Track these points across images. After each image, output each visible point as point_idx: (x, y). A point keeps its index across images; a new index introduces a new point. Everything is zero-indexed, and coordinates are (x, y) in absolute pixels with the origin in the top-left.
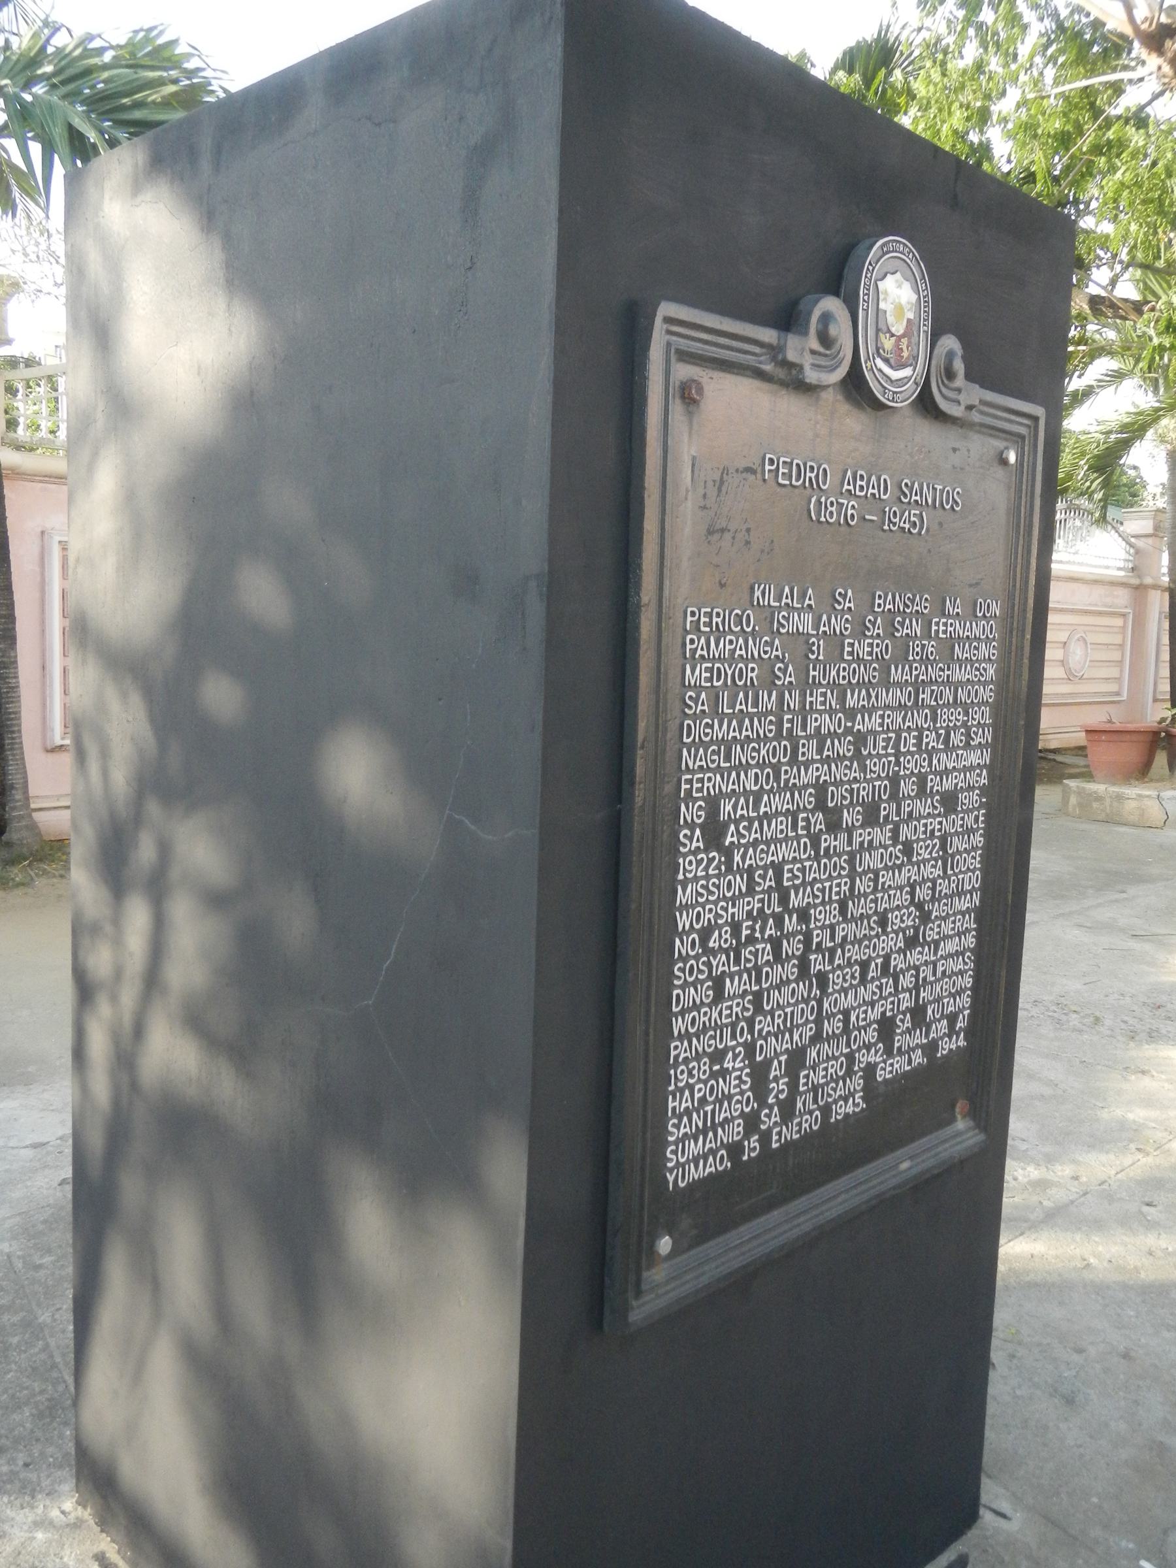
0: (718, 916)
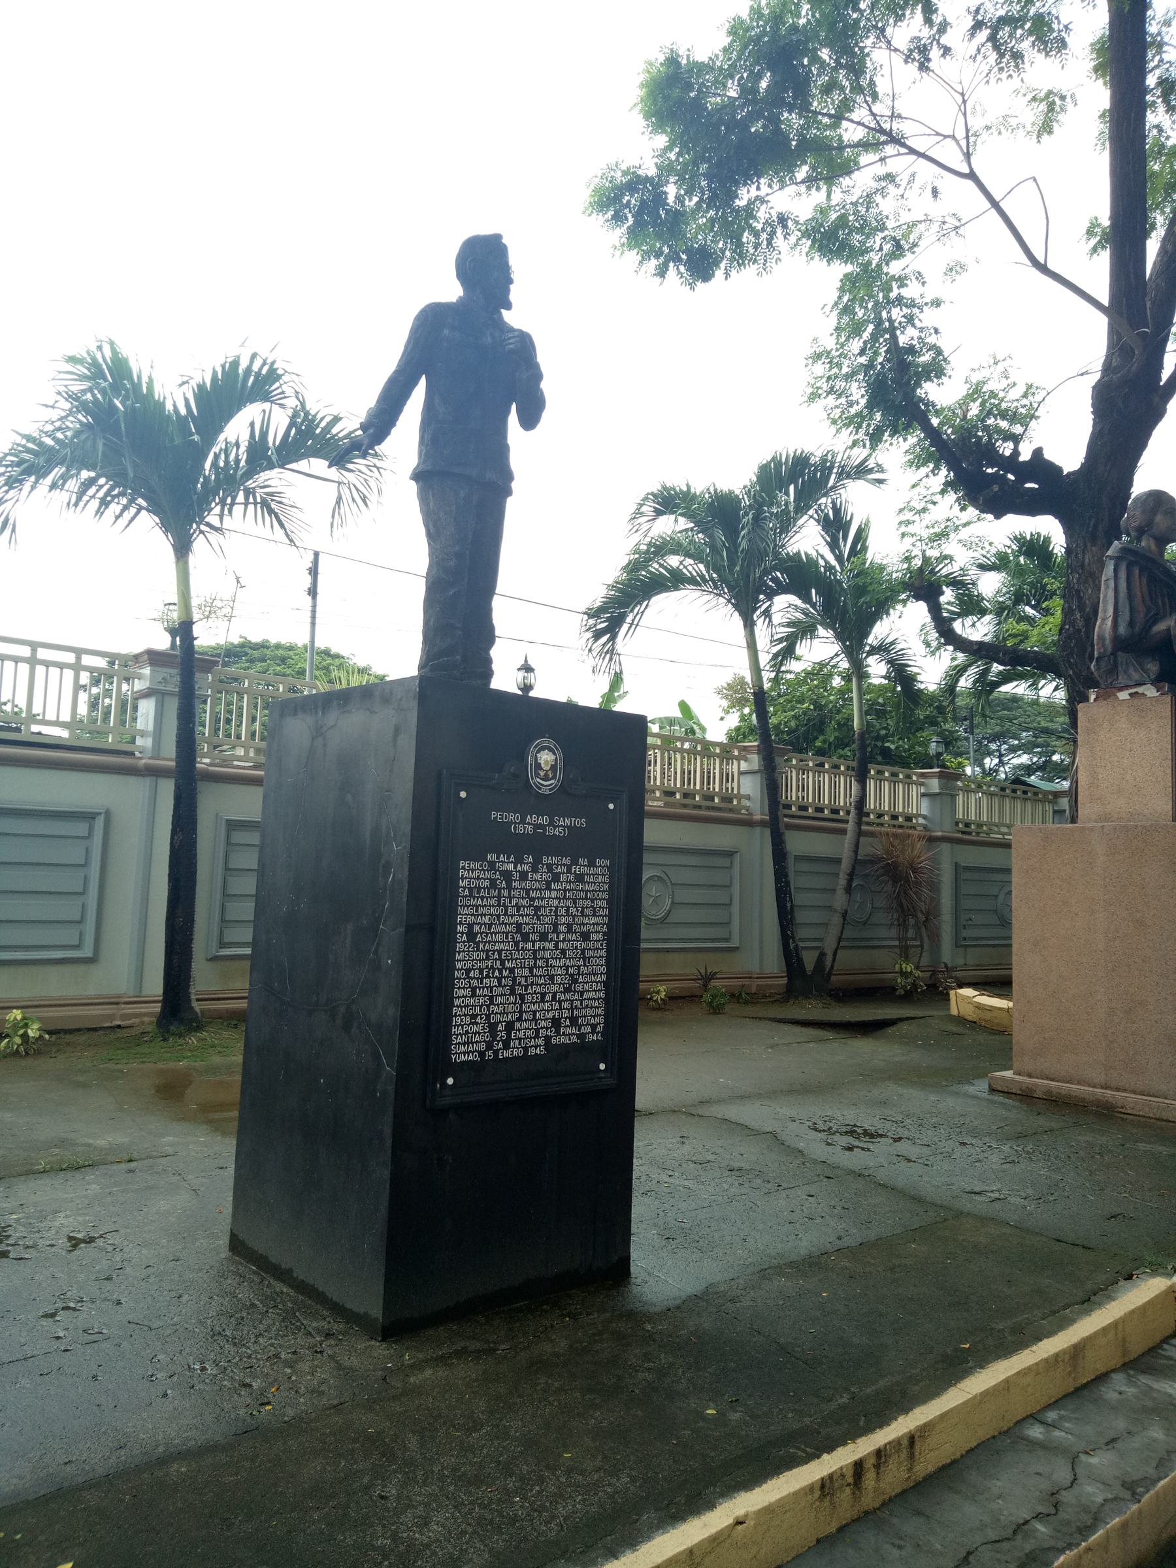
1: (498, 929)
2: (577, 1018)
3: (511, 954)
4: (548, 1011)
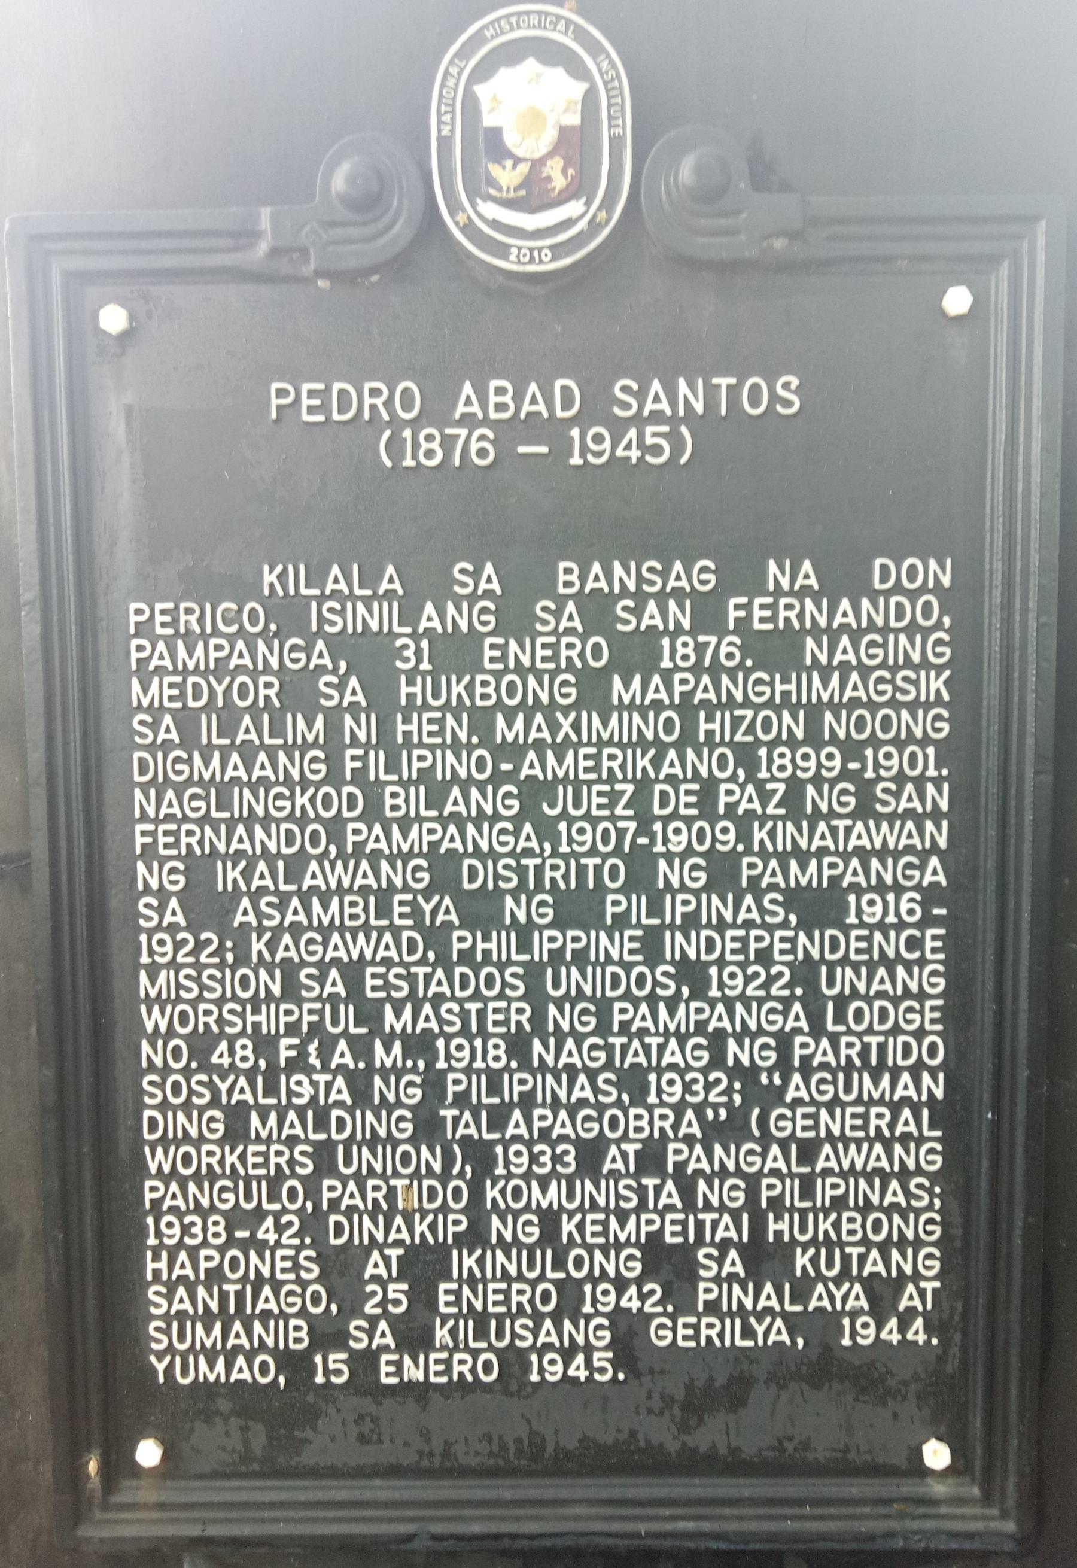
0: (220, 1020)
1: (340, 875)
2: (785, 1249)
3: (411, 979)
4: (623, 1217)
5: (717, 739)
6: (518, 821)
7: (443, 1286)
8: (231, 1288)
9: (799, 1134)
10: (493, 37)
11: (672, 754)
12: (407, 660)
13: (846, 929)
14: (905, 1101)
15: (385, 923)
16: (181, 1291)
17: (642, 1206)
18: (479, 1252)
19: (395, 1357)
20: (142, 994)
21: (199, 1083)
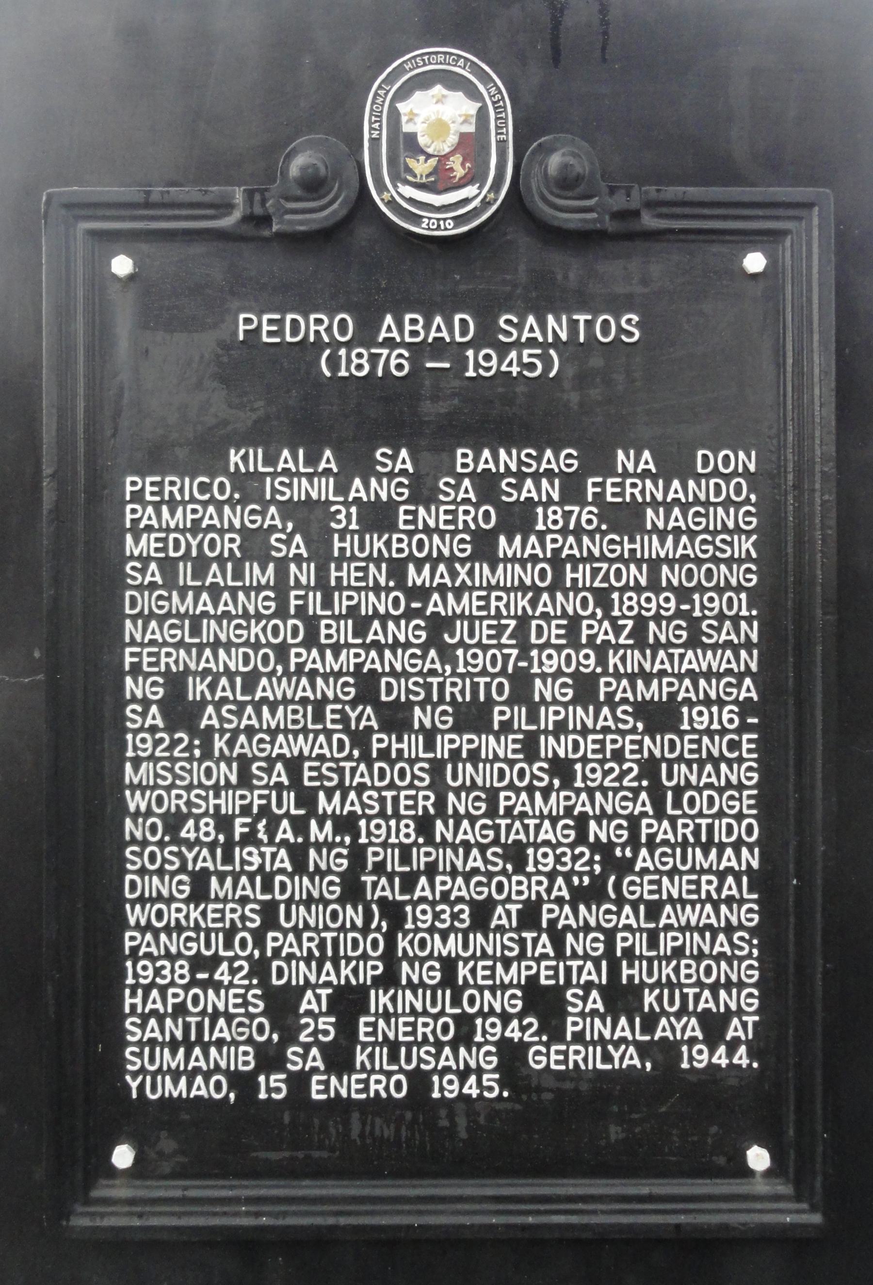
0: (189, 803)
1: (283, 689)
2: (636, 990)
3: (340, 771)
4: (507, 963)
5: (580, 585)
6: (425, 647)
7: (363, 1020)
8: (193, 1020)
9: (646, 896)
10: (411, 70)
11: (545, 597)
12: (339, 522)
13: (681, 734)
14: (729, 870)
15: (320, 727)
16: (153, 1022)
17: (522, 956)
18: (392, 991)
19: (325, 1077)
20: (127, 781)
21: (171, 853)
